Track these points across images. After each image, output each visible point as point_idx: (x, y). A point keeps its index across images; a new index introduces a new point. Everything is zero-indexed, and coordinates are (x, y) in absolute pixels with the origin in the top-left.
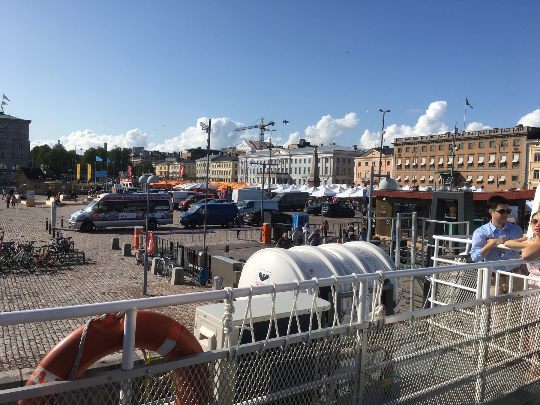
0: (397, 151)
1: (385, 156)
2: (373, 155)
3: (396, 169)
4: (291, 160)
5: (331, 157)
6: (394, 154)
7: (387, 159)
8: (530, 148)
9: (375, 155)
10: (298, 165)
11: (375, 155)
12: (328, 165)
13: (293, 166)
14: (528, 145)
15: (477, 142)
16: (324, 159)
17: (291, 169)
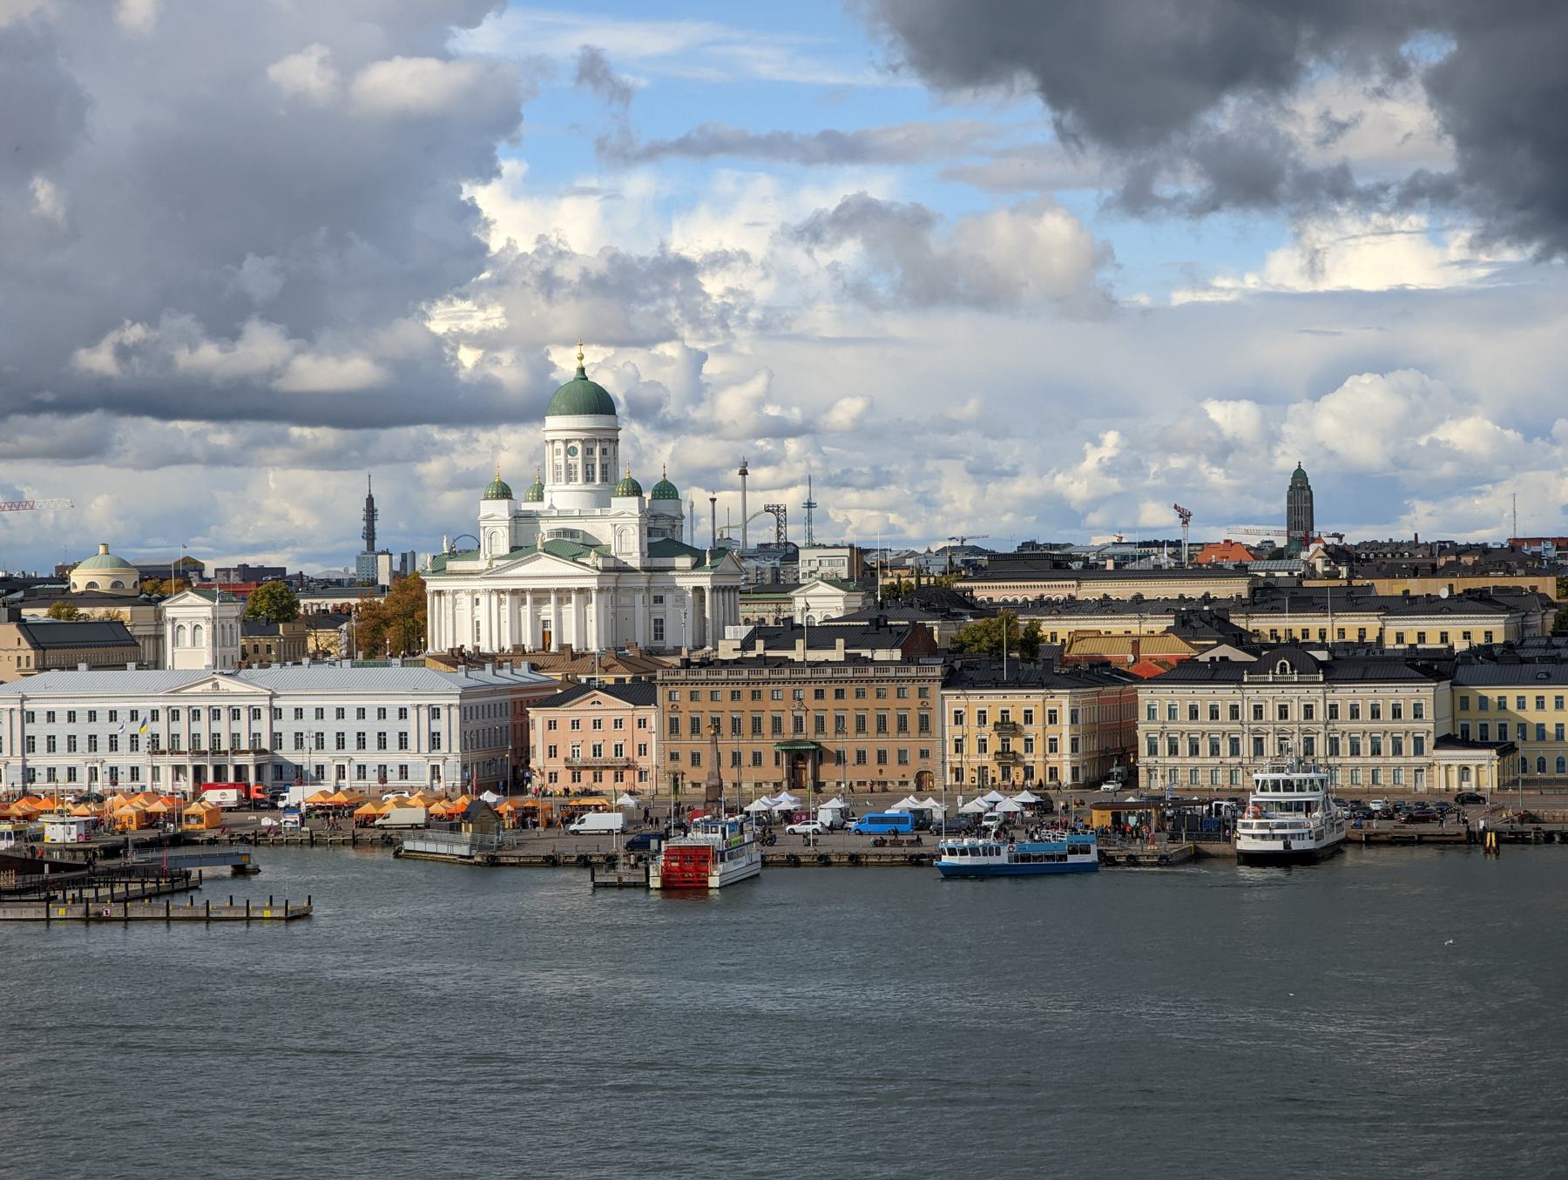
0: (667, 698)
1: (632, 706)
2: (593, 703)
3: (667, 737)
4: (277, 713)
5: (450, 706)
6: (659, 702)
7: (636, 713)
8: (946, 702)
9: (599, 703)
10: (309, 725)
11: (599, 703)
12: (440, 726)
13: (287, 726)
14: (943, 697)
15: (850, 689)
16: (424, 713)
17: (276, 739)
